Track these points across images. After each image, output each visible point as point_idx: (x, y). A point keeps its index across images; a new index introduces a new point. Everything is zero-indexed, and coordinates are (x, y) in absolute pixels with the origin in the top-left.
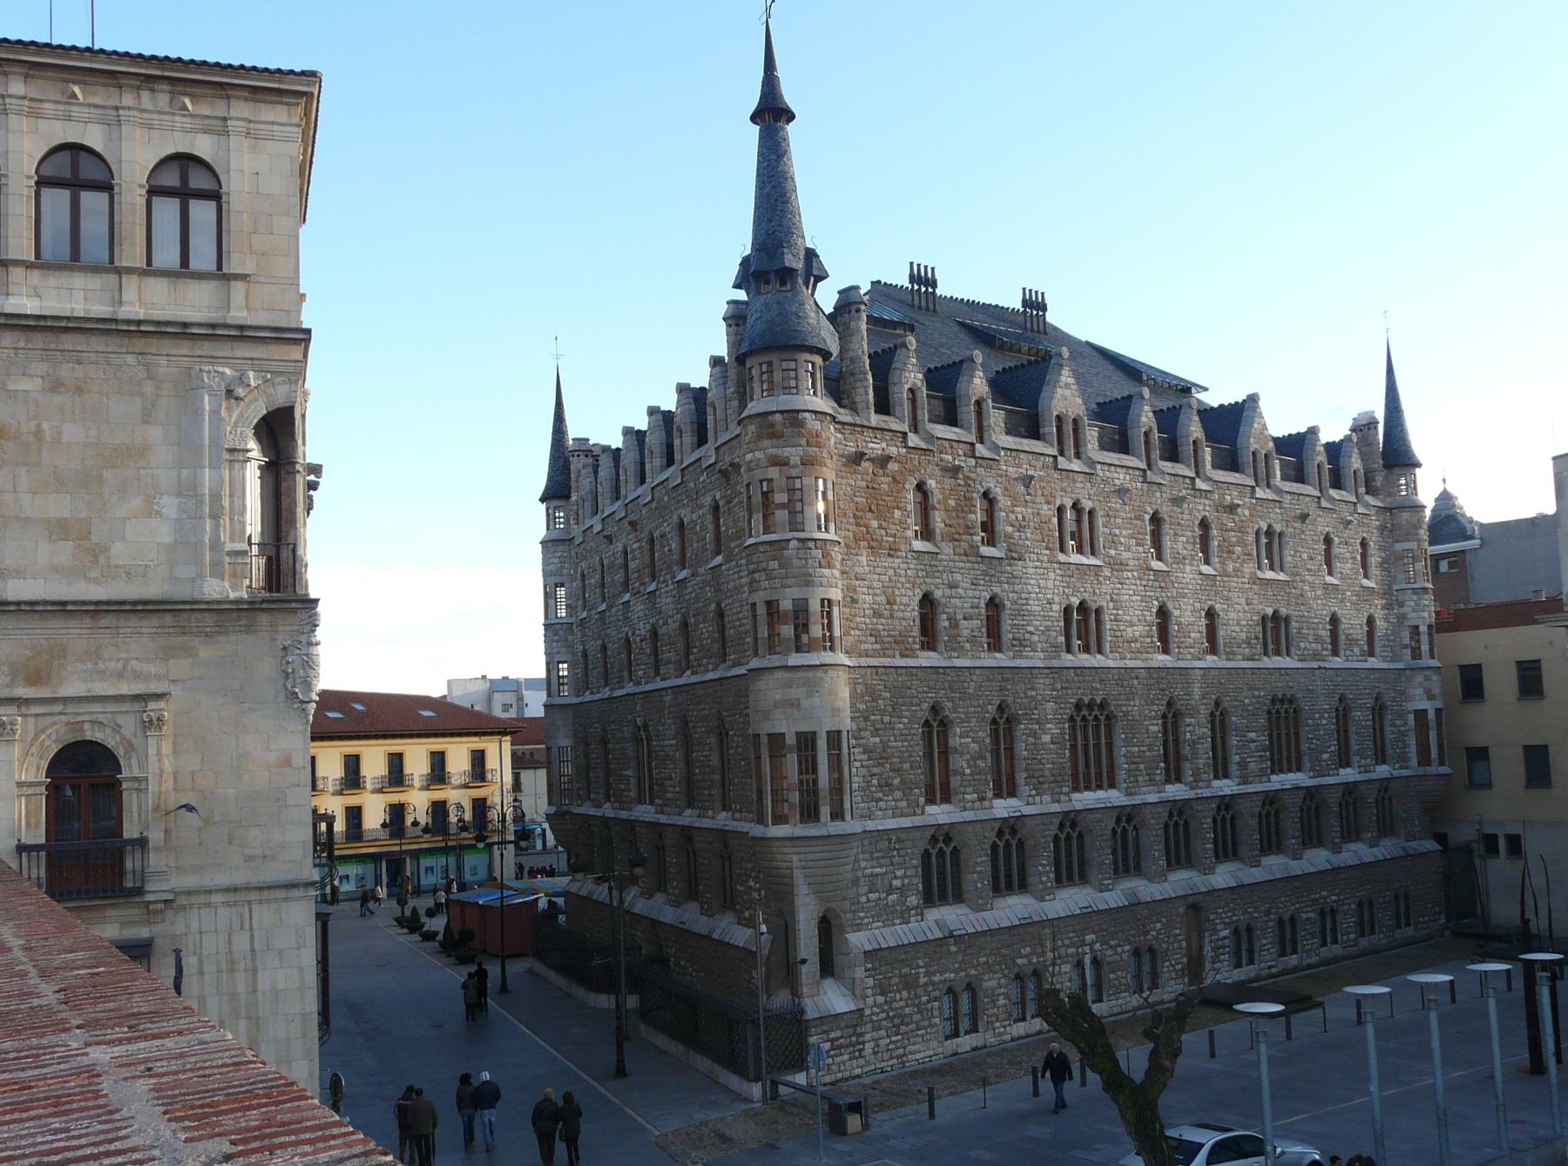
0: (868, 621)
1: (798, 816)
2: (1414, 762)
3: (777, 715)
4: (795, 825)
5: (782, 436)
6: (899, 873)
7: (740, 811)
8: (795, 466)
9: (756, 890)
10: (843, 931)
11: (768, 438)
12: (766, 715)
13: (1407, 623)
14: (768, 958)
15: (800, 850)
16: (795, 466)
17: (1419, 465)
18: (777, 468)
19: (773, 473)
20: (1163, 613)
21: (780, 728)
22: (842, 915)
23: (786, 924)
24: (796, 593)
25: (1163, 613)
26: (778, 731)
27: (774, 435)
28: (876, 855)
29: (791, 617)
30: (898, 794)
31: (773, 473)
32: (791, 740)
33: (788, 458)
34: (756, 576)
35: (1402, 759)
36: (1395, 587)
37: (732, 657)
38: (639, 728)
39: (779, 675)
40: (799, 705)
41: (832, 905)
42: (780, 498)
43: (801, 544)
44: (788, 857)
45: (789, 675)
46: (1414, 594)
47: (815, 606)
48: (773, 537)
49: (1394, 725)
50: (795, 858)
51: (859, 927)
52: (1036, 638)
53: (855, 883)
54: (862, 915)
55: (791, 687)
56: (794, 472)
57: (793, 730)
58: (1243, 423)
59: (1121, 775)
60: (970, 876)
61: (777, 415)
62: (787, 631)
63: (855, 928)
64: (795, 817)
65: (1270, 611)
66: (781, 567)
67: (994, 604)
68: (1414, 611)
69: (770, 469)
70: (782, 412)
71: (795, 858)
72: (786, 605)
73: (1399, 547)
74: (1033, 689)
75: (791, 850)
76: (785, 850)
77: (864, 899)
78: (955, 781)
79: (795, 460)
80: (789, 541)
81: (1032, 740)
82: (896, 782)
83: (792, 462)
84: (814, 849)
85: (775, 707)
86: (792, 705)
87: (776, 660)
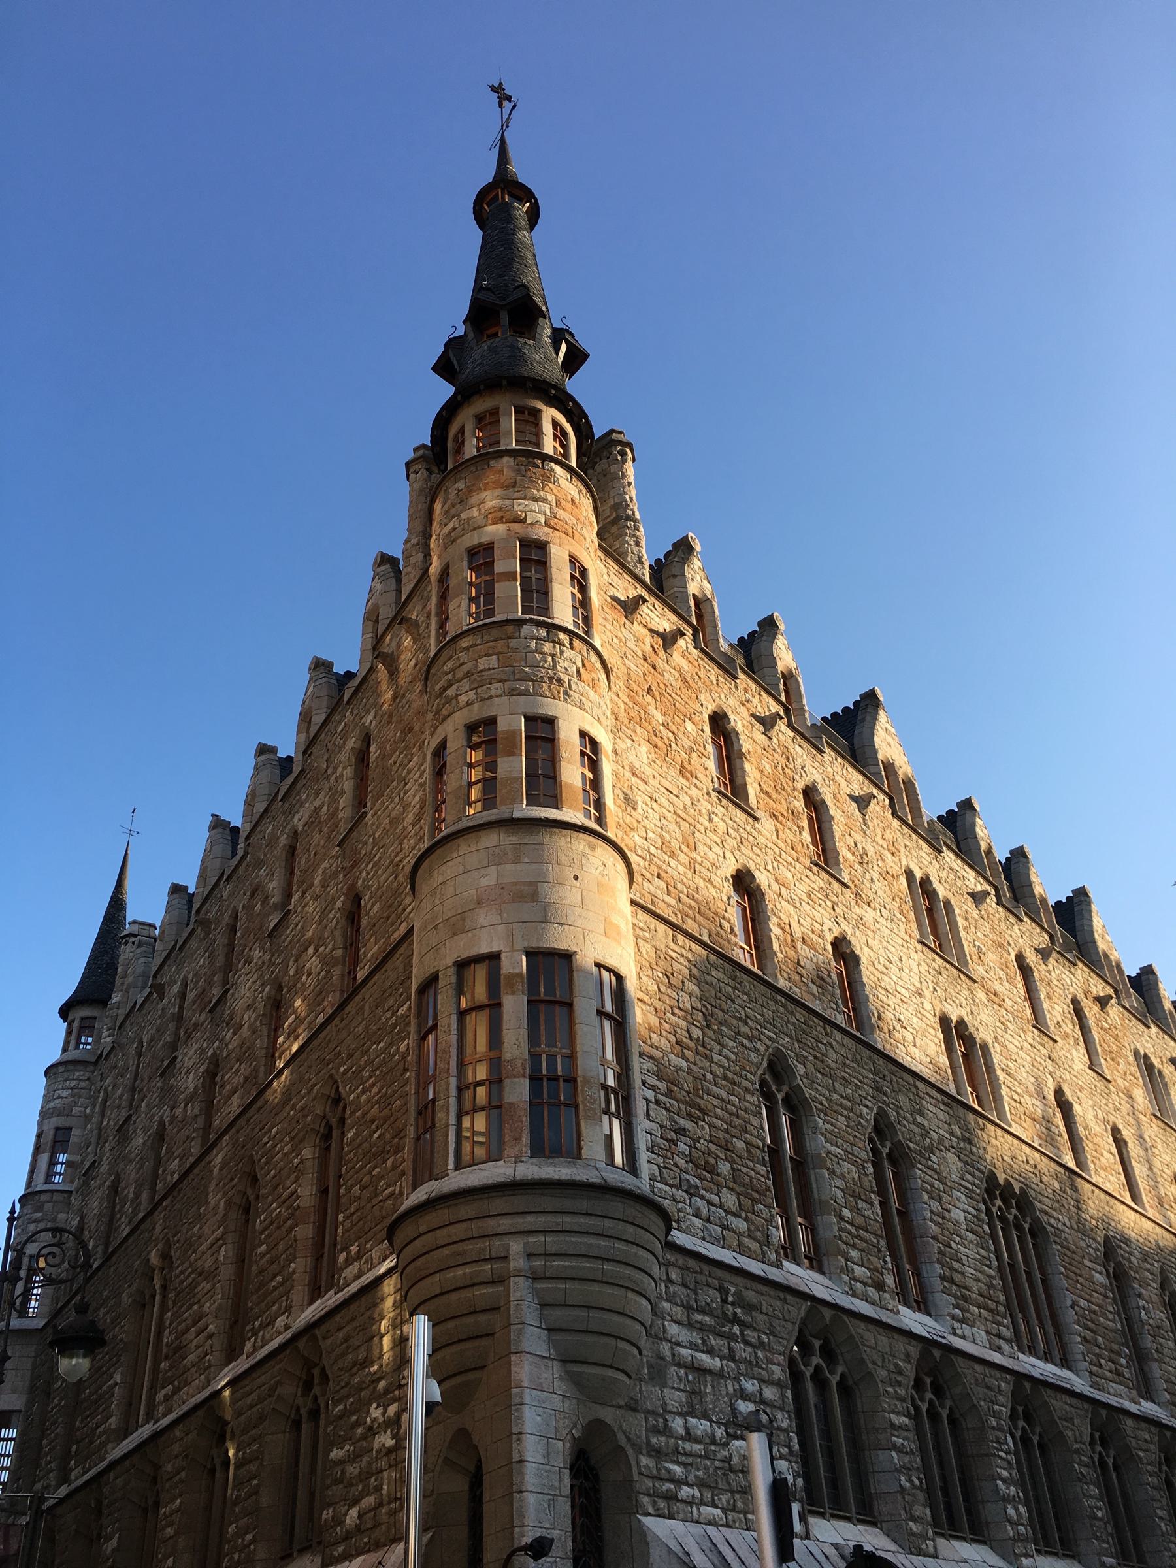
0: (653, 850)
1: (526, 1139)
3: (484, 917)
6: (750, 1386)
10: (636, 1509)
15: (529, 1221)
22: (630, 1451)
23: (479, 1467)
28: (698, 1317)
30: (730, 1200)
34: (451, 692)
39: (491, 839)
41: (607, 1415)
50: (516, 1247)
51: (670, 1506)
53: (658, 1374)
54: (677, 1469)
55: (517, 860)
57: (521, 944)
59: (1078, 1348)
60: (882, 1455)
63: (662, 1504)
64: (518, 1139)
71: (516, 1247)
74: (922, 1114)
75: (506, 1223)
77: (677, 1424)
78: (829, 1225)
81: (935, 1205)
82: (725, 1168)
85: (479, 903)
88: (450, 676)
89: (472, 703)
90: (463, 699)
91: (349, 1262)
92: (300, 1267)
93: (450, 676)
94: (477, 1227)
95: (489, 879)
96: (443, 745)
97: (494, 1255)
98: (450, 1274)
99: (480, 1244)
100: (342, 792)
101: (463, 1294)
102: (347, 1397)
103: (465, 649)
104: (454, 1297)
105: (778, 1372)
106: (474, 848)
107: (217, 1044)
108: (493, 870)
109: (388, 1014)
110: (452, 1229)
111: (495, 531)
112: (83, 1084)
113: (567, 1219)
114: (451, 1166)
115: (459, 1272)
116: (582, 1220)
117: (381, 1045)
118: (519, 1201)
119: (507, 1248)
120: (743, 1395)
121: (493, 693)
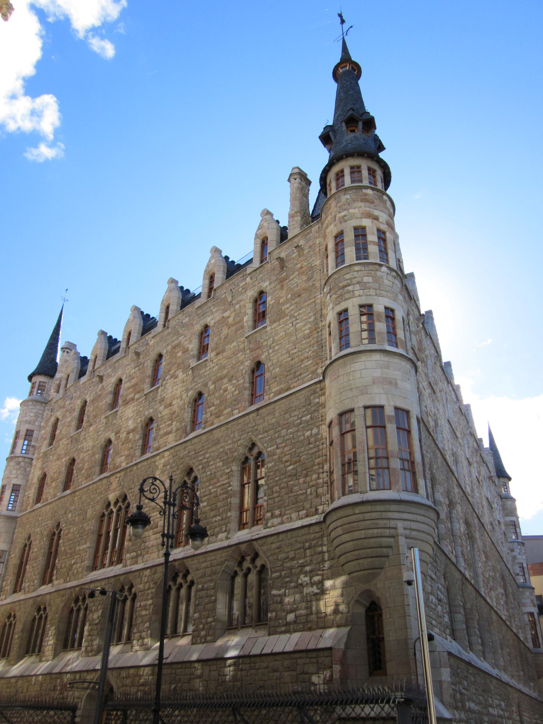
7: (280, 515)
9: (312, 584)
13: (516, 561)
14: (344, 653)
17: (509, 479)
29: (384, 316)
32: (389, 411)
38: (109, 504)
39: (377, 357)
40: (396, 384)
43: (389, 272)
44: (392, 523)
46: (519, 545)
55: (388, 368)
57: (392, 404)
68: (519, 554)
72: (379, 308)
75: (396, 515)
76: (390, 515)
84: (419, 518)
85: (374, 383)
86: (390, 383)
88: (349, 281)
89: (362, 296)
90: (357, 293)
91: (273, 516)
92: (233, 514)
93: (349, 281)
94: (384, 515)
95: (378, 373)
96: (346, 310)
97: (391, 526)
98: (371, 531)
99: (385, 521)
100: (245, 314)
101: (376, 540)
102: (283, 570)
103: (356, 271)
104: (372, 540)
106: (369, 359)
107: (151, 410)
109: (295, 418)
110: (372, 514)
111: (366, 222)
112: (40, 412)
113: (418, 517)
114: (368, 489)
115: (375, 531)
116: (423, 518)
117: (290, 430)
118: (402, 507)
119: (397, 525)
121: (371, 293)
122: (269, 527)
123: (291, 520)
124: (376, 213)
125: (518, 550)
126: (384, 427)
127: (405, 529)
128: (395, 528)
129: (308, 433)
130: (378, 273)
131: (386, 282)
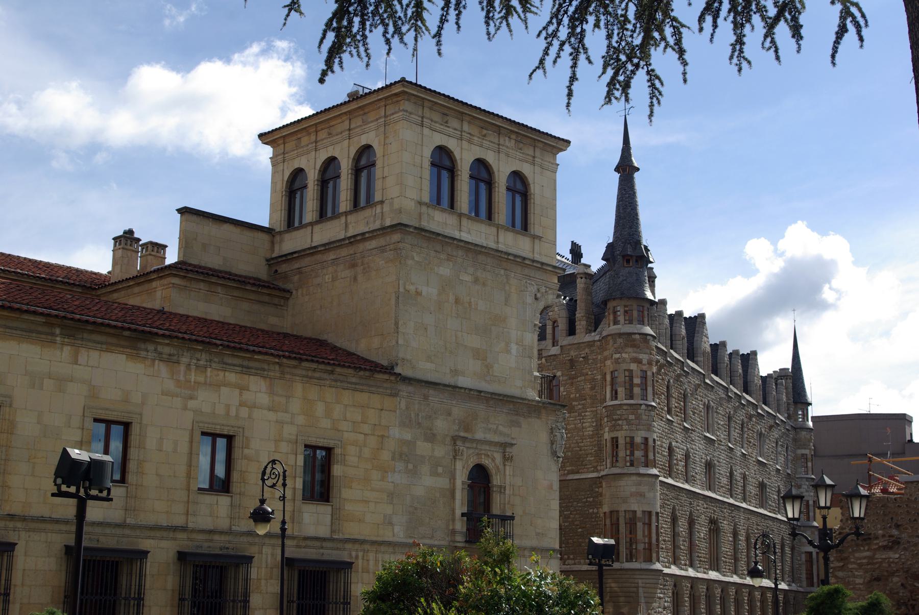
1: (642, 558)
2: (804, 583)
4: (641, 563)
5: (639, 347)
6: (666, 599)
7: (573, 559)
8: (644, 365)
11: (631, 347)
12: (625, 500)
15: (643, 577)
16: (644, 365)
17: (811, 404)
18: (635, 365)
19: (633, 366)
20: (731, 473)
21: (634, 507)
24: (643, 434)
25: (731, 473)
26: (632, 509)
27: (634, 346)
31: (633, 366)
32: (639, 514)
33: (642, 359)
34: (620, 422)
35: (800, 581)
36: (797, 476)
37: (567, 468)
39: (634, 478)
40: (644, 496)
42: (637, 381)
44: (636, 581)
45: (639, 479)
46: (807, 481)
47: (651, 442)
48: (632, 402)
49: (797, 560)
50: (640, 581)
52: (698, 477)
55: (640, 485)
56: (644, 368)
57: (641, 509)
58: (750, 367)
61: (637, 335)
62: (638, 454)
65: (761, 479)
66: (636, 418)
67: (687, 456)
68: (807, 491)
69: (632, 364)
70: (640, 334)
71: (640, 581)
72: (638, 440)
73: (800, 452)
75: (638, 577)
76: (635, 576)
79: (645, 361)
80: (641, 405)
83: (644, 362)
84: (650, 577)
86: (641, 495)
87: (632, 470)
91: (569, 558)
95: (633, 489)
105: (670, 594)
108: (635, 487)
117: (579, 504)
120: (665, 602)
122: (567, 565)
123: (580, 564)
124: (641, 356)
125: (806, 487)
126: (636, 524)
127: (642, 583)
128: (638, 583)
129: (591, 511)
130: (639, 411)
131: (644, 417)
